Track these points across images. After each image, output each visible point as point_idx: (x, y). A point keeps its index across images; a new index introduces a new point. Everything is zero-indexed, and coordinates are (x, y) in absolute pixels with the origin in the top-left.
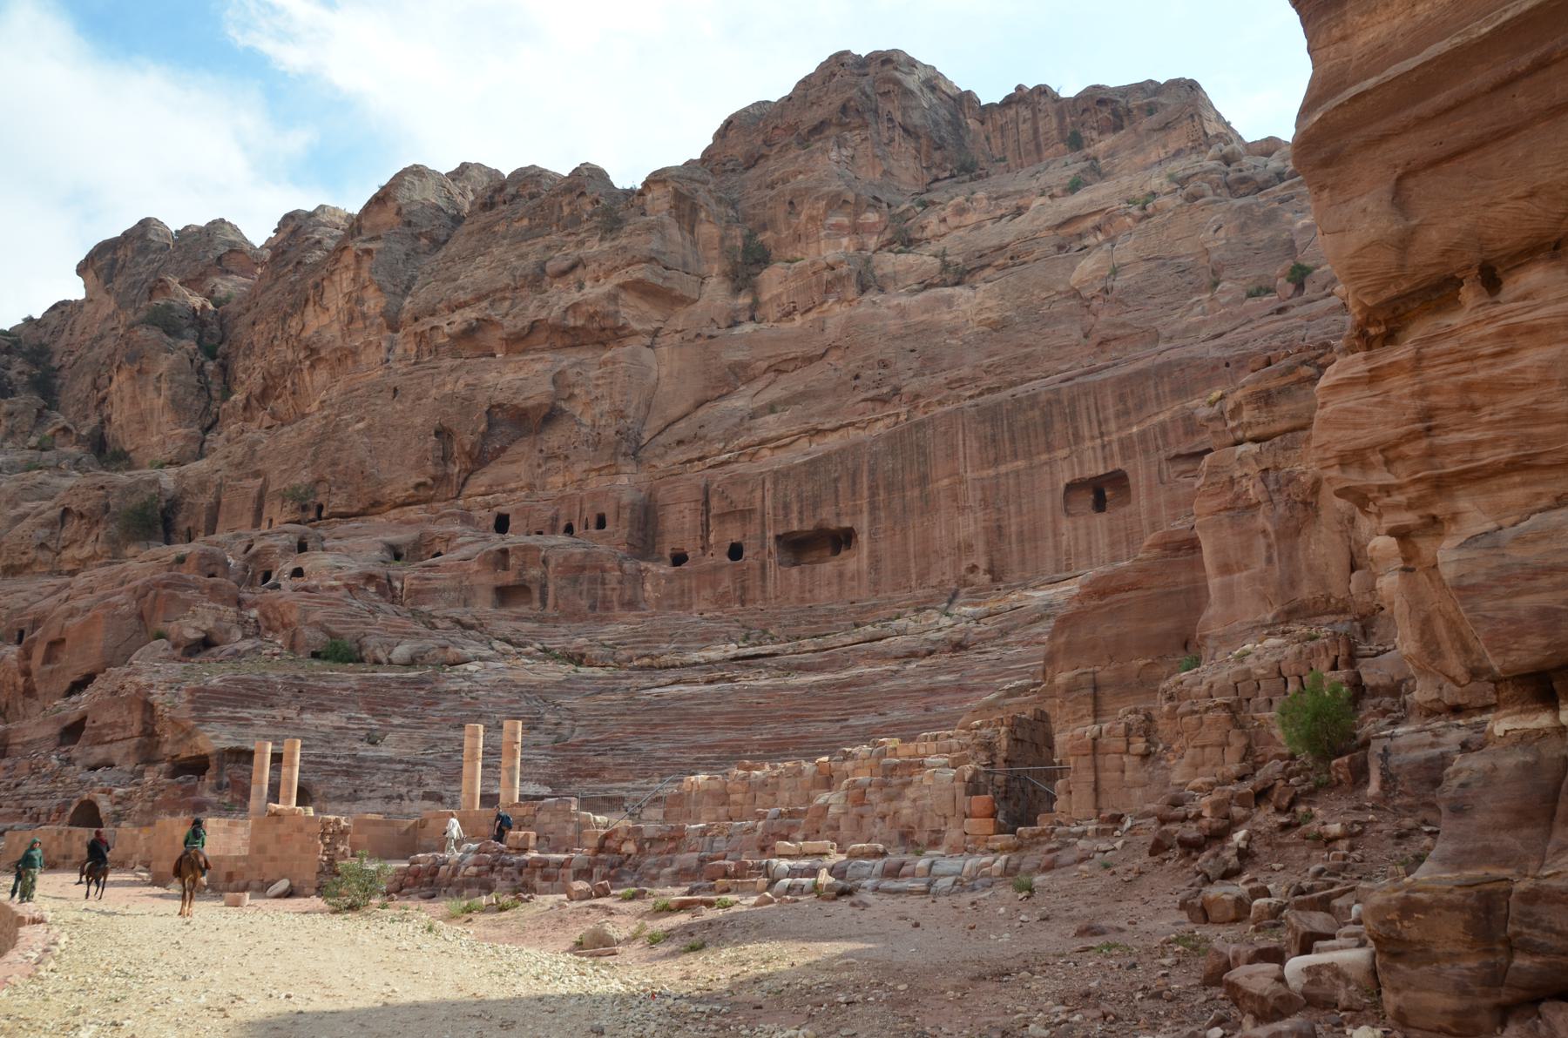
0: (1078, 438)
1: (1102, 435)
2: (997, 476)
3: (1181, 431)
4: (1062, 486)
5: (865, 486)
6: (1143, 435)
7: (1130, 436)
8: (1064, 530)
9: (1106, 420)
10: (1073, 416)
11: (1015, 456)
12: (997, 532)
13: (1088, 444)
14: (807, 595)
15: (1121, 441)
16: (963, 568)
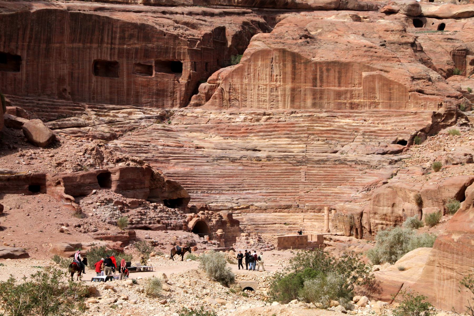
0: (102, 41)
1: (112, 43)
2: (73, 48)
3: (143, 55)
4: (93, 60)
5: (28, 37)
6: (128, 51)
7: (123, 49)
8: (93, 81)
9: (115, 38)
10: (103, 29)
11: (80, 42)
12: (71, 74)
13: (105, 45)
14: (4, 88)
15: (119, 49)
16: (61, 89)
